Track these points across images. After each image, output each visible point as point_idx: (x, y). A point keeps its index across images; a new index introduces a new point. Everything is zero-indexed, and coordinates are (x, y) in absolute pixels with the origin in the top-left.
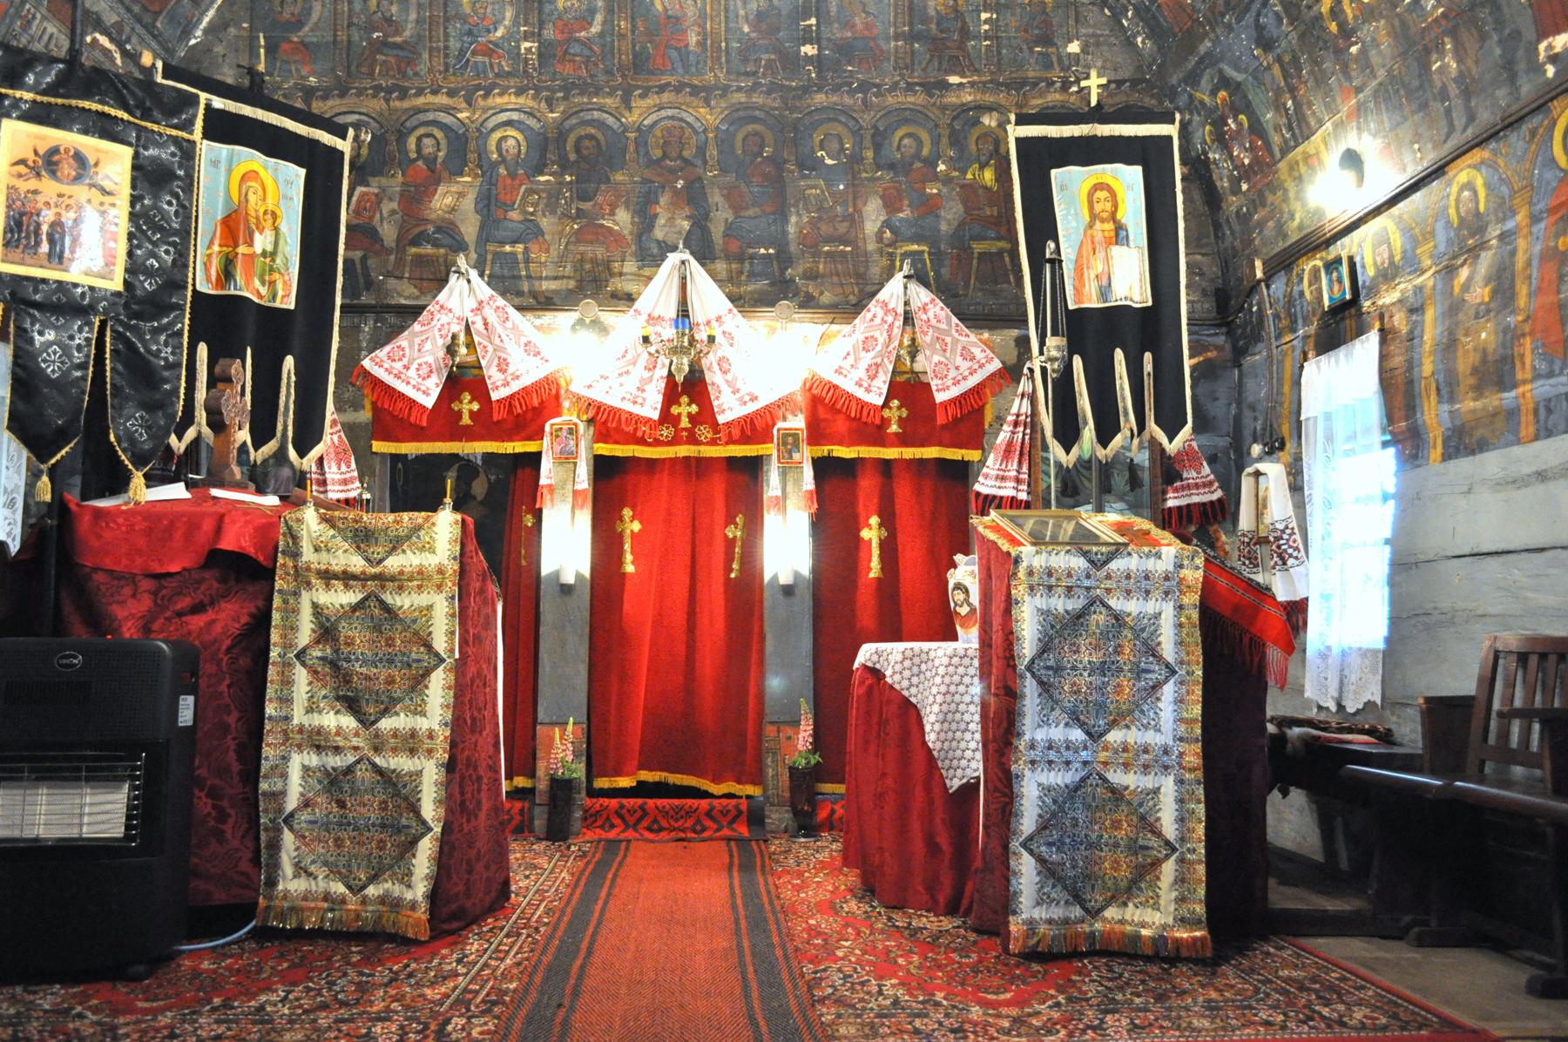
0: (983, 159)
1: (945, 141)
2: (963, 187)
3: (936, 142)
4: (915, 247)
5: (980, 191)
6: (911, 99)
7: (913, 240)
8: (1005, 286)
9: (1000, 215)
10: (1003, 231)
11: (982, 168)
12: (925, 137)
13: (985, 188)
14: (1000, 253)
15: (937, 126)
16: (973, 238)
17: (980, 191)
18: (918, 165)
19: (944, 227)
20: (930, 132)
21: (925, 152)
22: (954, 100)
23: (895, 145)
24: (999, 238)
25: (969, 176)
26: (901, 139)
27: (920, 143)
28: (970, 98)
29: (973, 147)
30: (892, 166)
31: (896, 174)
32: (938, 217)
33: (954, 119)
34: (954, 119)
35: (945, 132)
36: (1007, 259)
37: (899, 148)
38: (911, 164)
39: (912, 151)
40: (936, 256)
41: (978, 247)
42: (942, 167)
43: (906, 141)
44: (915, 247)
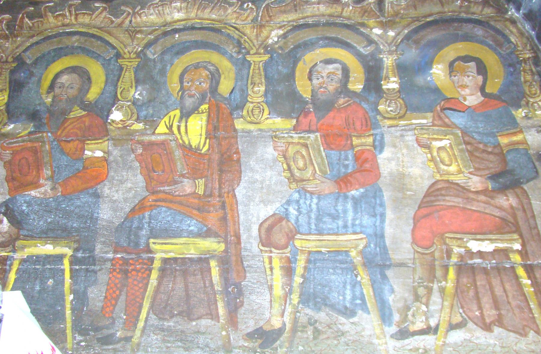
0: (189, 102)
1: (128, 76)
2: (148, 146)
3: (114, 78)
4: (48, 249)
5: (178, 153)
6: (86, 20)
7: (51, 234)
8: (205, 322)
9: (209, 195)
10: (213, 219)
11: (186, 115)
12: (97, 71)
13: (187, 149)
14: (202, 261)
15: (118, 56)
16: (154, 234)
17: (178, 153)
18: (77, 112)
19: (105, 214)
20: (106, 64)
21: (93, 94)
22: (153, 18)
23: (46, 84)
24: (208, 234)
25: (162, 129)
26: (57, 76)
27: (86, 78)
28: (177, 16)
29: (174, 84)
30: (34, 116)
31: (38, 129)
32: (97, 196)
33: (149, 45)
34: (149, 45)
35: (130, 64)
36: (215, 272)
37: (52, 87)
38: (64, 113)
39: (72, 92)
40: (85, 263)
41: (162, 250)
42: (116, 116)
43: (65, 79)
44: (48, 249)
